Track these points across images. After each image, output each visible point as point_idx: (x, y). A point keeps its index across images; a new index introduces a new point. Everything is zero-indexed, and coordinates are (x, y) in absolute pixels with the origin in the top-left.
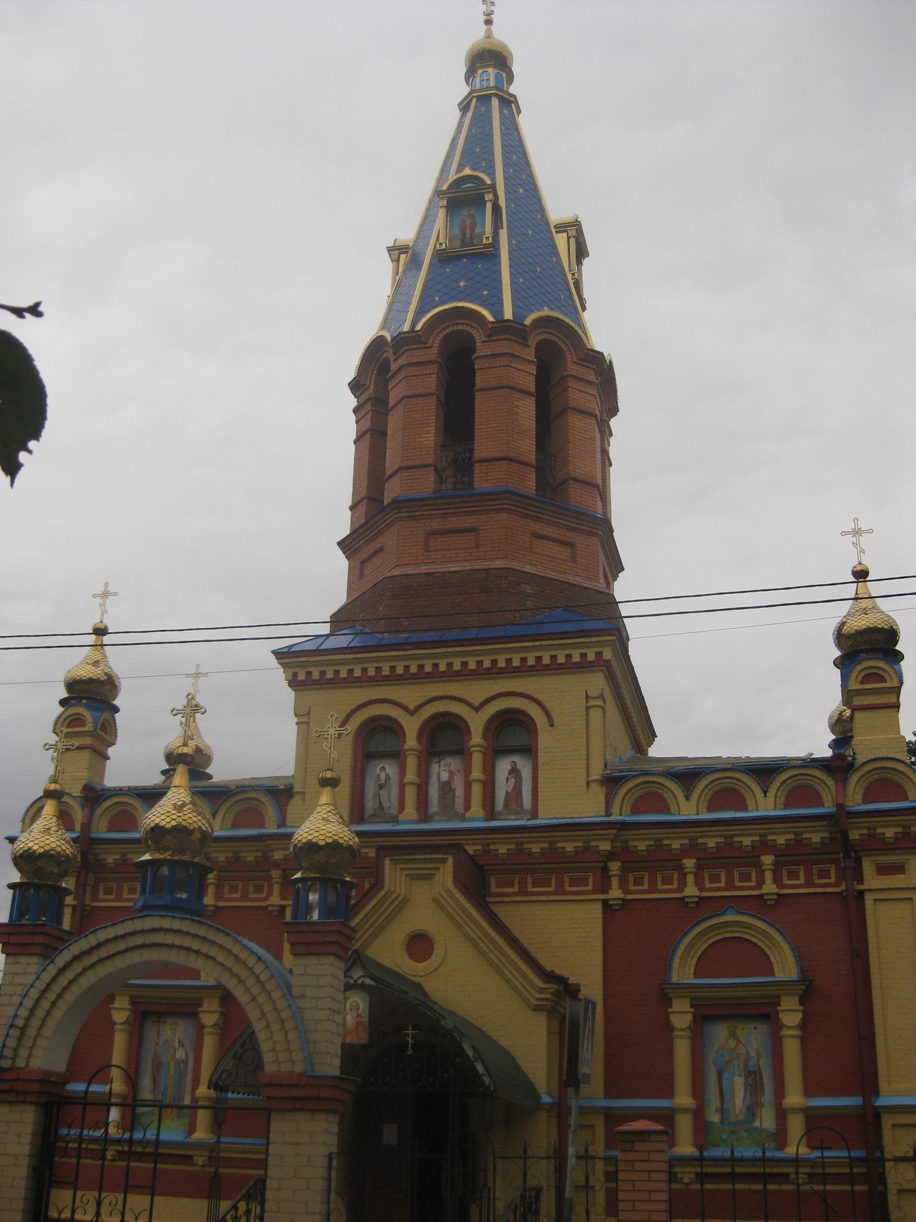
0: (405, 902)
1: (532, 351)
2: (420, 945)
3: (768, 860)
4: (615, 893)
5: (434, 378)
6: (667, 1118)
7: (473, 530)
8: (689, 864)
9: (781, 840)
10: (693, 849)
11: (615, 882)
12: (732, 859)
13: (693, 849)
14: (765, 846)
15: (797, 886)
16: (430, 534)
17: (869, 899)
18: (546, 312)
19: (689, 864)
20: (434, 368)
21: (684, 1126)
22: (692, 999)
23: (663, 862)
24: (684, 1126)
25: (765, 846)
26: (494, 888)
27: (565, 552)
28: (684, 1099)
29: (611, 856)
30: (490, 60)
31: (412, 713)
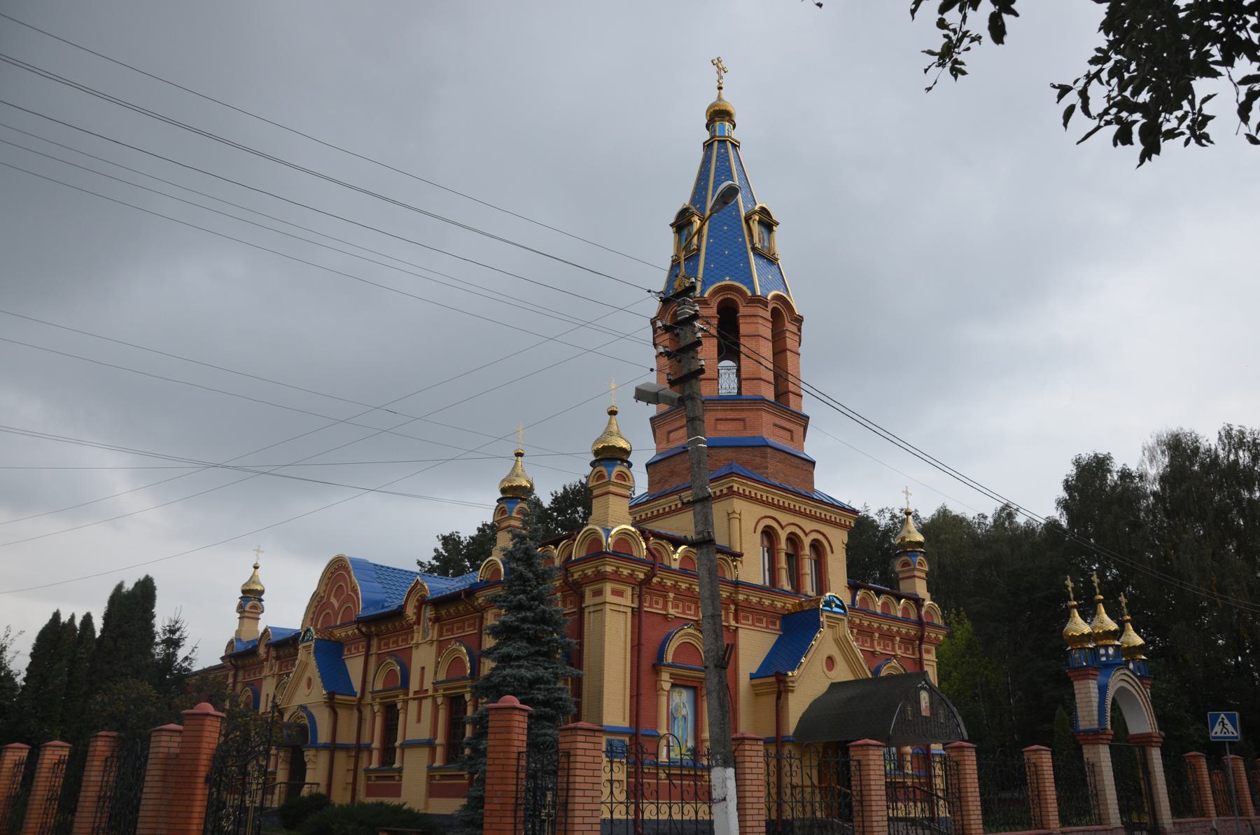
1: (715, 310)
18: (727, 281)
27: (739, 425)
30: (719, 115)
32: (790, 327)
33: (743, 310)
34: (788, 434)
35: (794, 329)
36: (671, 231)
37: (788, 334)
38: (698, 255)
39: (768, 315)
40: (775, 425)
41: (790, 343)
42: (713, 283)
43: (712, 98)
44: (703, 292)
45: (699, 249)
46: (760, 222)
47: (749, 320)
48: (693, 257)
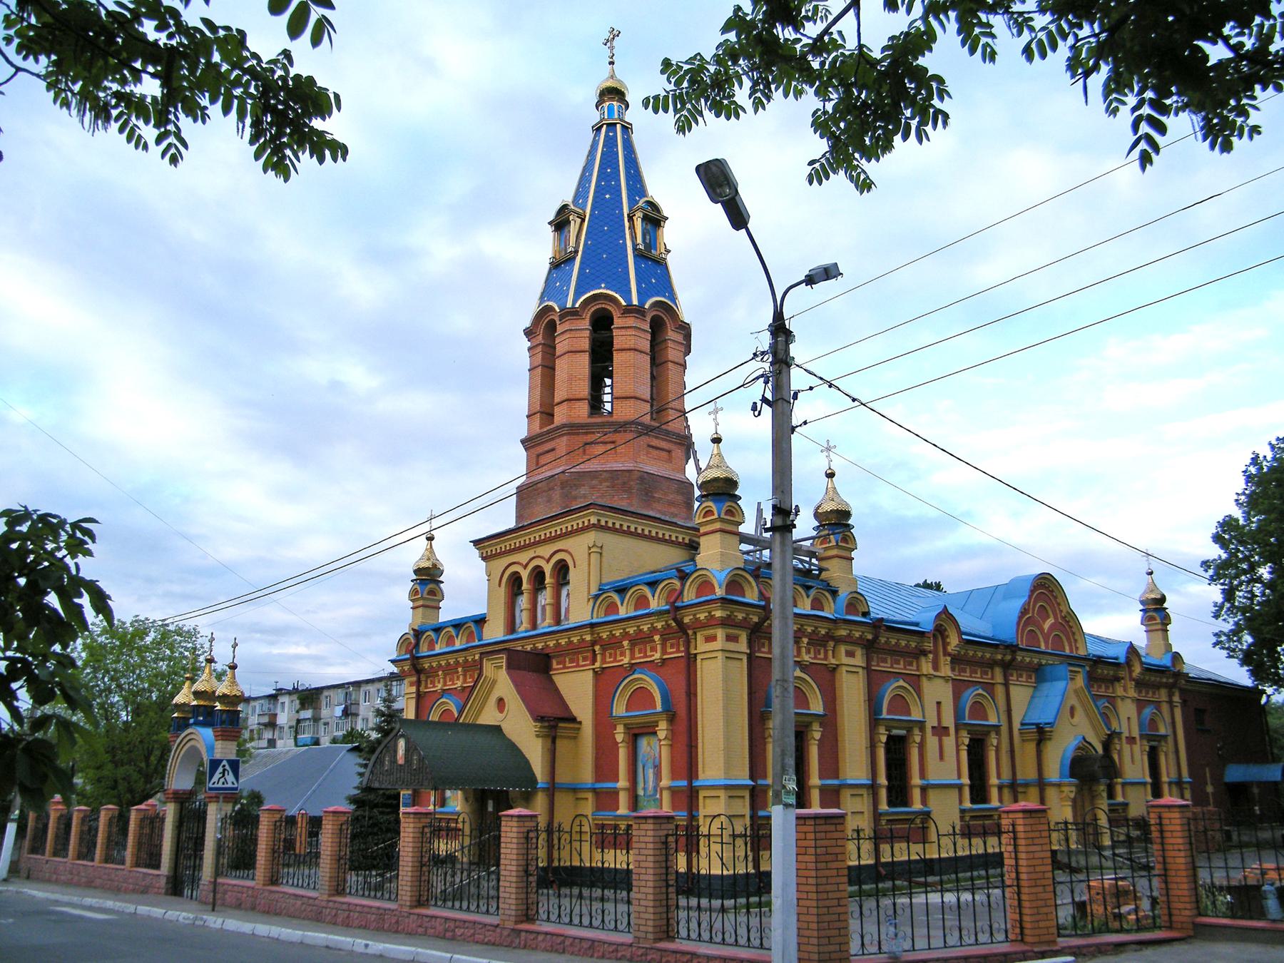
0: (494, 682)
2: (501, 703)
3: (657, 638)
4: (597, 665)
5: (540, 355)
6: (615, 793)
7: (553, 450)
8: (625, 643)
9: (659, 625)
10: (626, 635)
11: (599, 657)
12: (640, 640)
13: (626, 635)
14: (654, 630)
15: (672, 653)
16: (538, 456)
17: (699, 657)
19: (625, 643)
20: (540, 348)
21: (623, 798)
22: (625, 725)
23: (612, 645)
24: (623, 798)
25: (654, 630)
26: (555, 666)
28: (623, 783)
29: (594, 643)
31: (525, 567)
32: (672, 334)
33: (618, 322)
34: (664, 454)
35: (679, 338)
36: (550, 229)
37: (670, 344)
38: (574, 258)
39: (647, 327)
40: (649, 446)
41: (673, 353)
42: (585, 293)
43: (601, 78)
44: (574, 301)
45: (576, 252)
46: (646, 218)
47: (624, 332)
48: (570, 260)
